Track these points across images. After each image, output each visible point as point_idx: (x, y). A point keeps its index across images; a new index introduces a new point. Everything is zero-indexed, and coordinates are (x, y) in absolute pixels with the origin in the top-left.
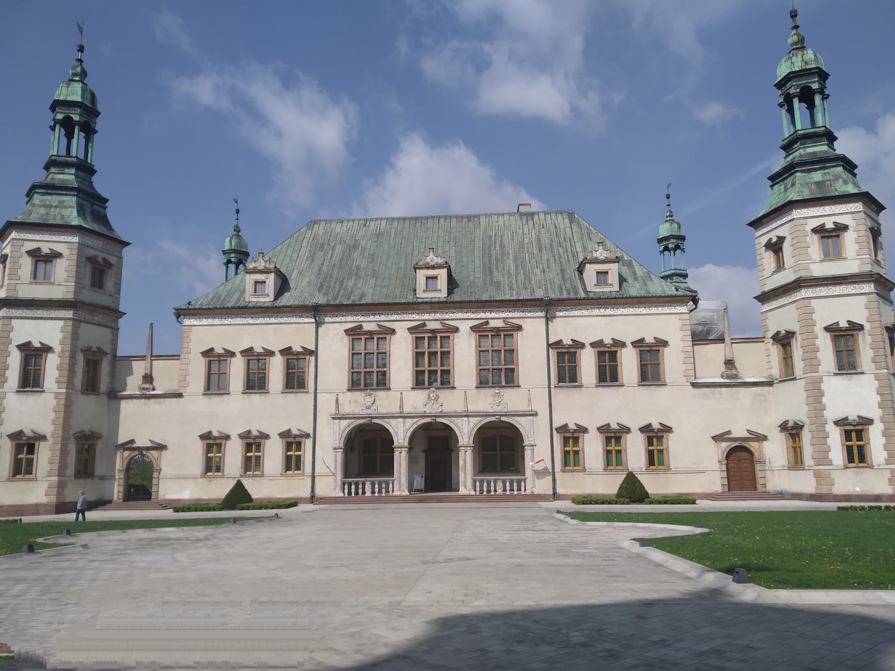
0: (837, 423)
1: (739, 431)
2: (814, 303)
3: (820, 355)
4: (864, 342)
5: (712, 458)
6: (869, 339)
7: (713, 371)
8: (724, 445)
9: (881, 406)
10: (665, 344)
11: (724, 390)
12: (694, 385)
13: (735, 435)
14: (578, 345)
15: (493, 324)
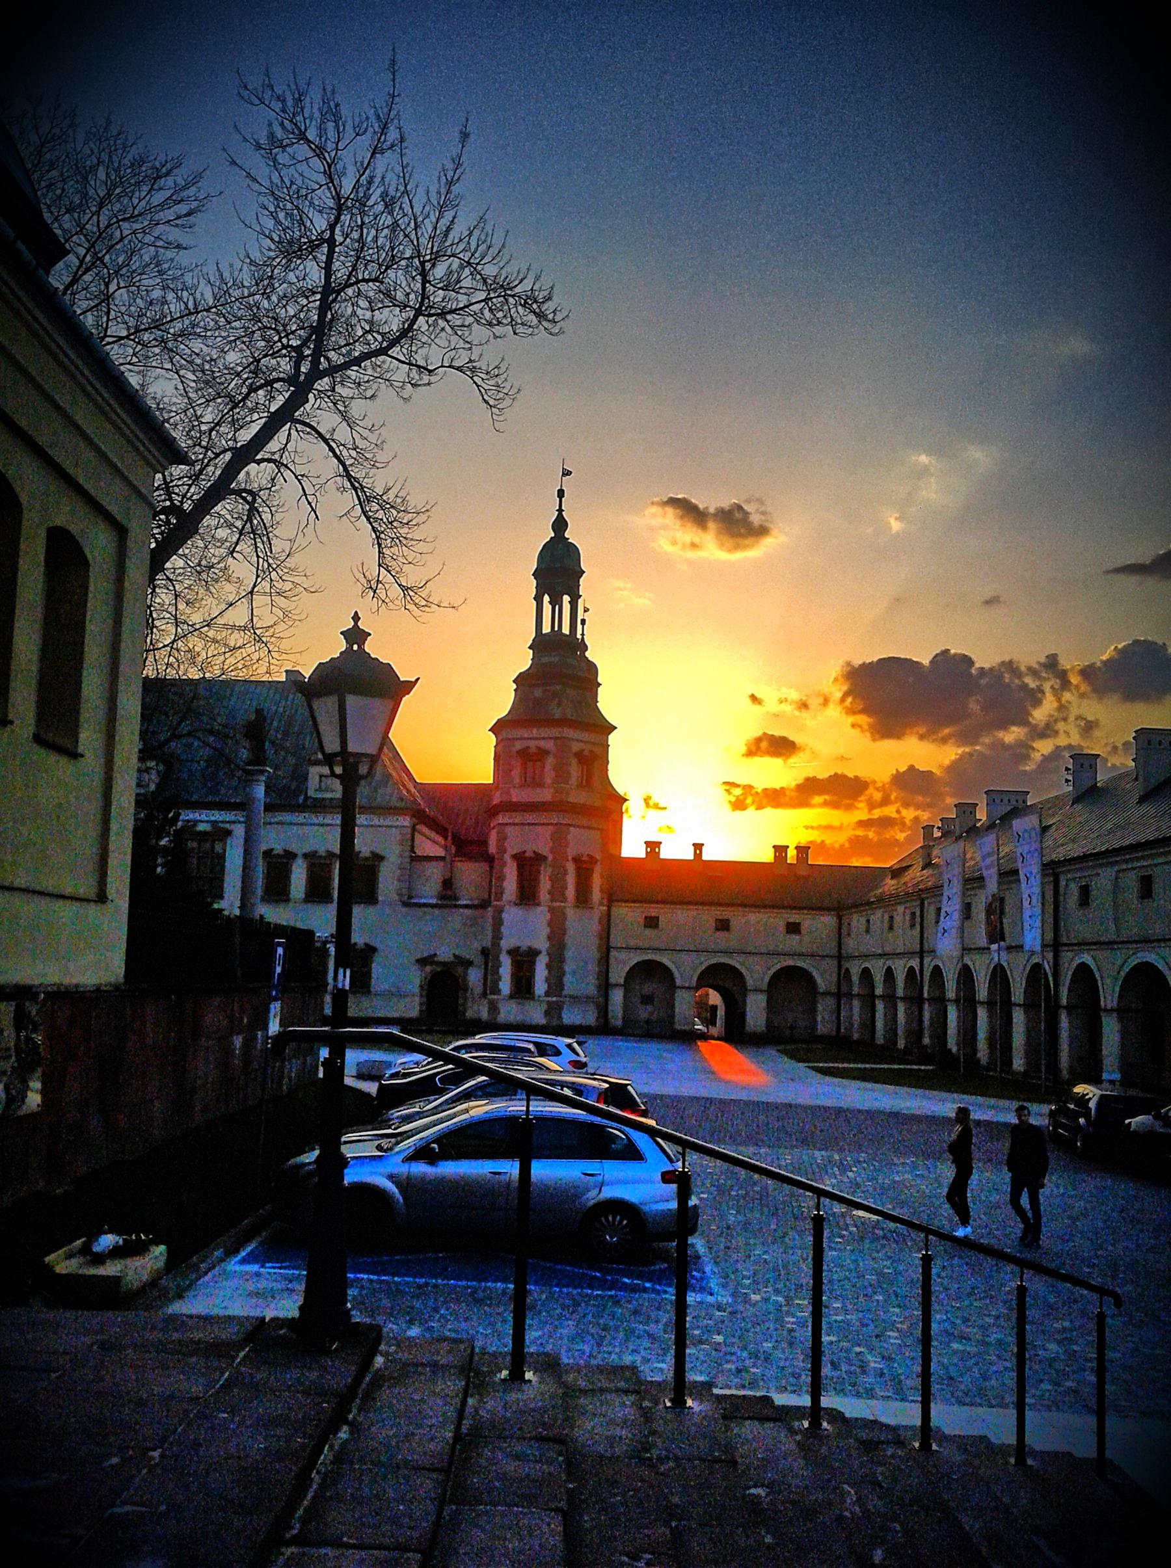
0: (509, 952)
1: (445, 954)
2: (509, 829)
3: (505, 884)
4: (545, 870)
5: (414, 980)
6: (549, 870)
7: (429, 890)
8: (428, 968)
9: (549, 938)
10: (382, 858)
11: (437, 911)
12: (405, 904)
13: (440, 959)
14: (290, 856)
15: (201, 827)
